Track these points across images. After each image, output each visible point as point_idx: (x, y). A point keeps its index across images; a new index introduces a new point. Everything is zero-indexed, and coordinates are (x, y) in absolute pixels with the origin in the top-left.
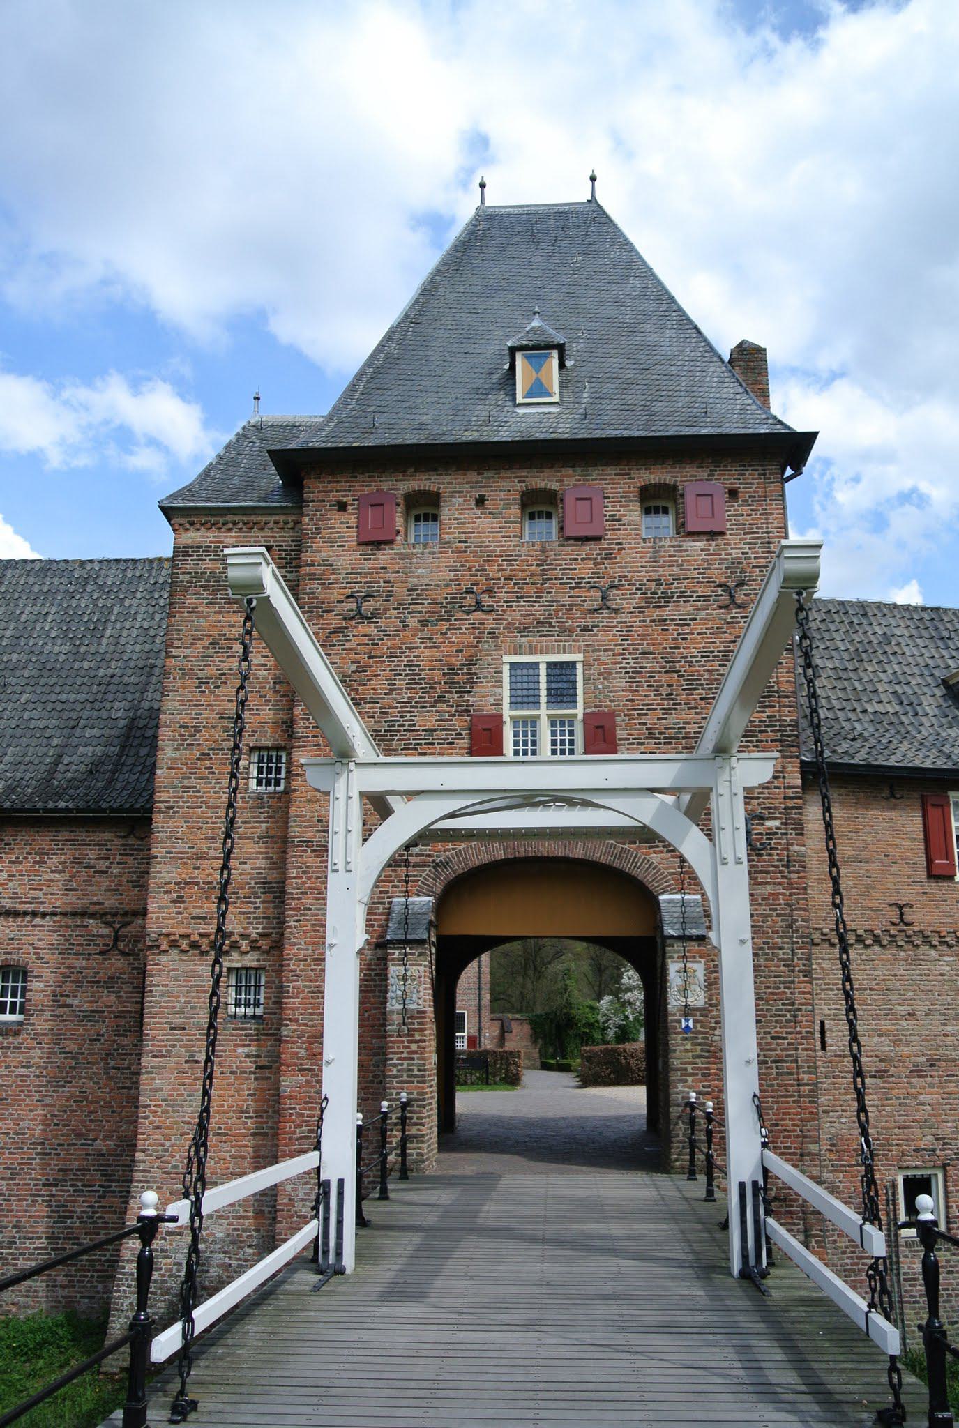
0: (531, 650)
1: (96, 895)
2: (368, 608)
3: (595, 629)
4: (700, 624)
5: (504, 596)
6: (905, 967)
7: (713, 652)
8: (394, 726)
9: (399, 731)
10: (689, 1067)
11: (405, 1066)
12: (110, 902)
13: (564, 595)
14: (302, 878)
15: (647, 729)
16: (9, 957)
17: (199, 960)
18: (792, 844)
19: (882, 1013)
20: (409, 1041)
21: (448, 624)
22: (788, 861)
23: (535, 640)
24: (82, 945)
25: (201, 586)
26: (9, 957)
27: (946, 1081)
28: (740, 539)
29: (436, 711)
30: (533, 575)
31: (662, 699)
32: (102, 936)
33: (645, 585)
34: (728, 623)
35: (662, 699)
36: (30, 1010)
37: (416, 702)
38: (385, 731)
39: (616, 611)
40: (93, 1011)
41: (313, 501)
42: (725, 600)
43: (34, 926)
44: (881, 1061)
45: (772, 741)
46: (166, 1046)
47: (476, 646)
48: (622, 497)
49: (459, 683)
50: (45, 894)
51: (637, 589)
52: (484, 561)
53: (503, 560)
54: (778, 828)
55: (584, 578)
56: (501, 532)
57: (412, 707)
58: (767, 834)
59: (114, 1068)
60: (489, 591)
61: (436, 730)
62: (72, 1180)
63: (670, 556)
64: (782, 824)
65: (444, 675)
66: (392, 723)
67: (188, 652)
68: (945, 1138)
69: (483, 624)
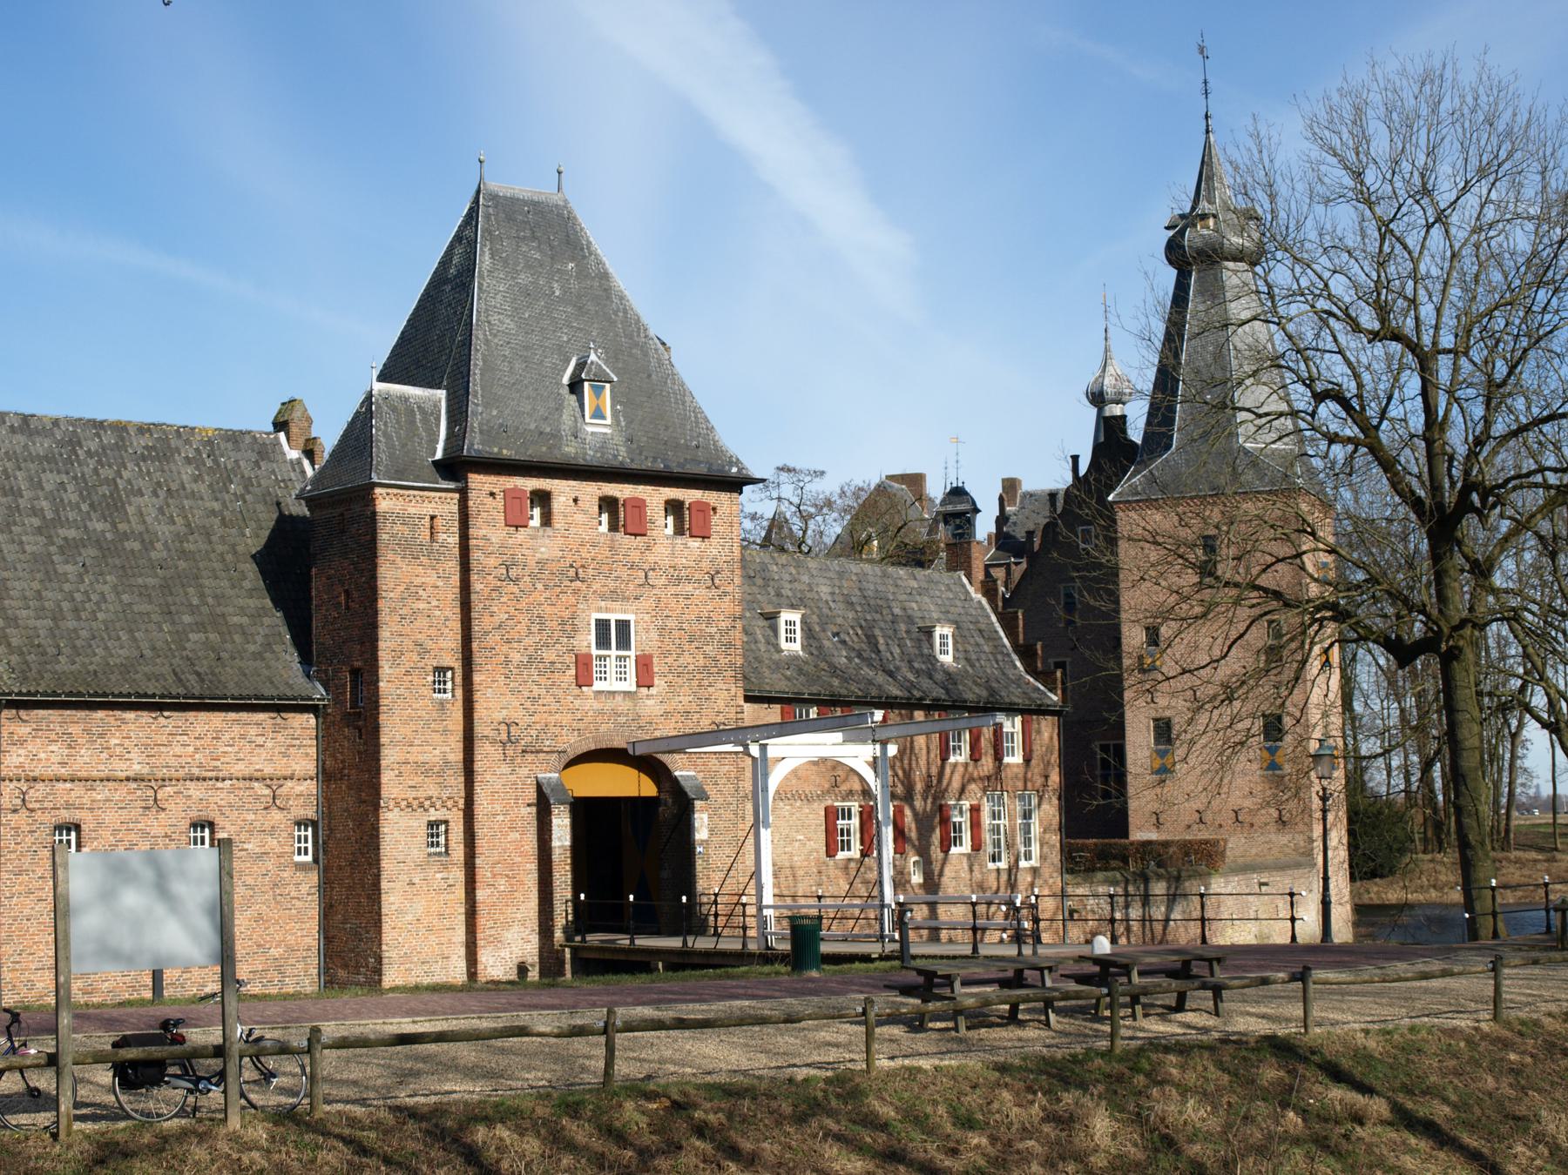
0: (607, 610)
2: (513, 573)
5: (591, 572)
12: (268, 770)
13: (624, 573)
21: (559, 590)
23: (609, 604)
42: (709, 583)
60: (583, 566)
66: (530, 657)
67: (392, 595)
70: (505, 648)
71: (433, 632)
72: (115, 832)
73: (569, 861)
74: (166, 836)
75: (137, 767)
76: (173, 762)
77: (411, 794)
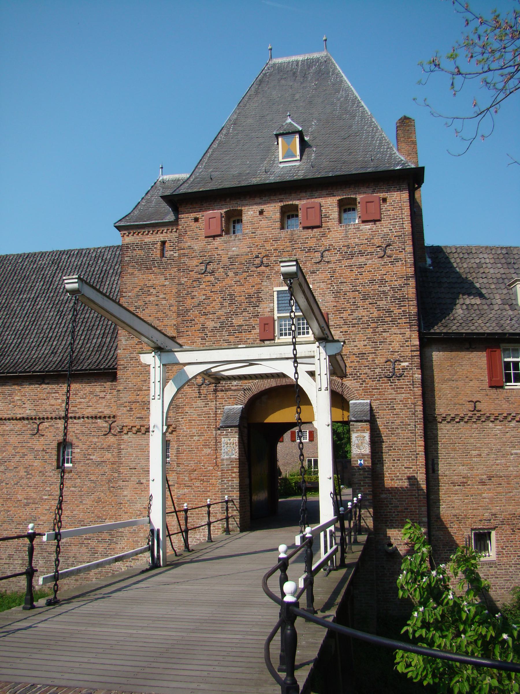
1: (101, 408)
2: (210, 268)
3: (317, 272)
4: (369, 267)
5: (273, 259)
6: (476, 432)
7: (375, 280)
8: (223, 324)
9: (225, 327)
10: (362, 482)
11: (230, 484)
12: (107, 412)
14: (183, 398)
15: (343, 320)
17: (141, 437)
18: (415, 374)
19: (465, 454)
20: (231, 473)
22: (413, 382)
24: (95, 431)
25: (135, 262)
27: (497, 487)
28: (388, 223)
29: (243, 316)
30: (287, 247)
31: (351, 305)
32: (104, 427)
33: (341, 248)
34: (383, 265)
35: (351, 305)
36: (74, 462)
37: (234, 312)
38: (219, 327)
39: (328, 262)
40: (102, 462)
41: (183, 218)
42: (382, 254)
43: (74, 423)
44: (463, 478)
45: (405, 323)
46: (128, 476)
47: (261, 284)
48: (330, 205)
49: (253, 302)
50: (78, 409)
51: (338, 251)
52: (264, 242)
53: (273, 241)
54: (407, 366)
55: (312, 247)
56: (272, 227)
57: (231, 315)
58: (402, 369)
59: (112, 487)
61: (243, 325)
62: (96, 537)
63: (353, 234)
64: (410, 364)
65: (246, 298)
67: (130, 294)
68: (496, 515)
69: (264, 273)
70: (202, 319)
71: (160, 315)
72: (15, 448)
73: (236, 470)
74: (43, 450)
75: (27, 411)
76: (49, 408)
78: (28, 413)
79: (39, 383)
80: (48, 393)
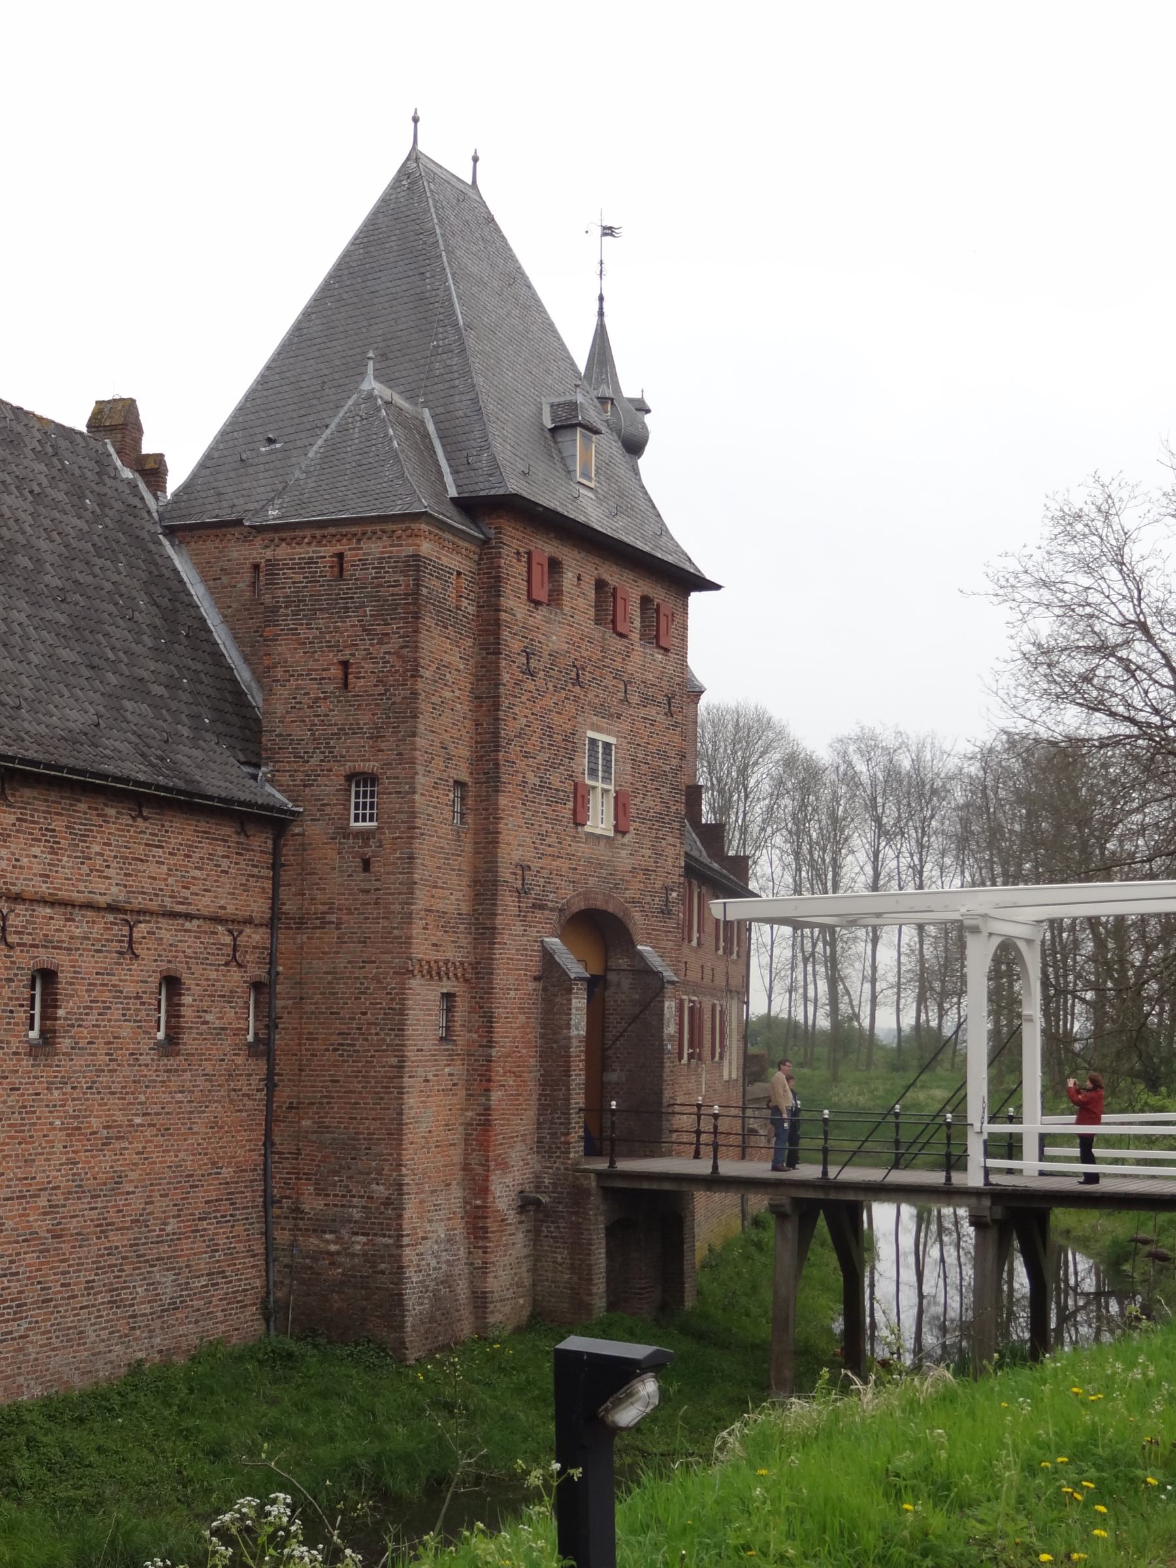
0: (598, 729)
13: (609, 682)
16: (170, 965)
26: (170, 965)
43: (186, 931)
74: (138, 997)
77: (432, 956)
78: (116, 893)
79: (133, 814)
80: (146, 845)
